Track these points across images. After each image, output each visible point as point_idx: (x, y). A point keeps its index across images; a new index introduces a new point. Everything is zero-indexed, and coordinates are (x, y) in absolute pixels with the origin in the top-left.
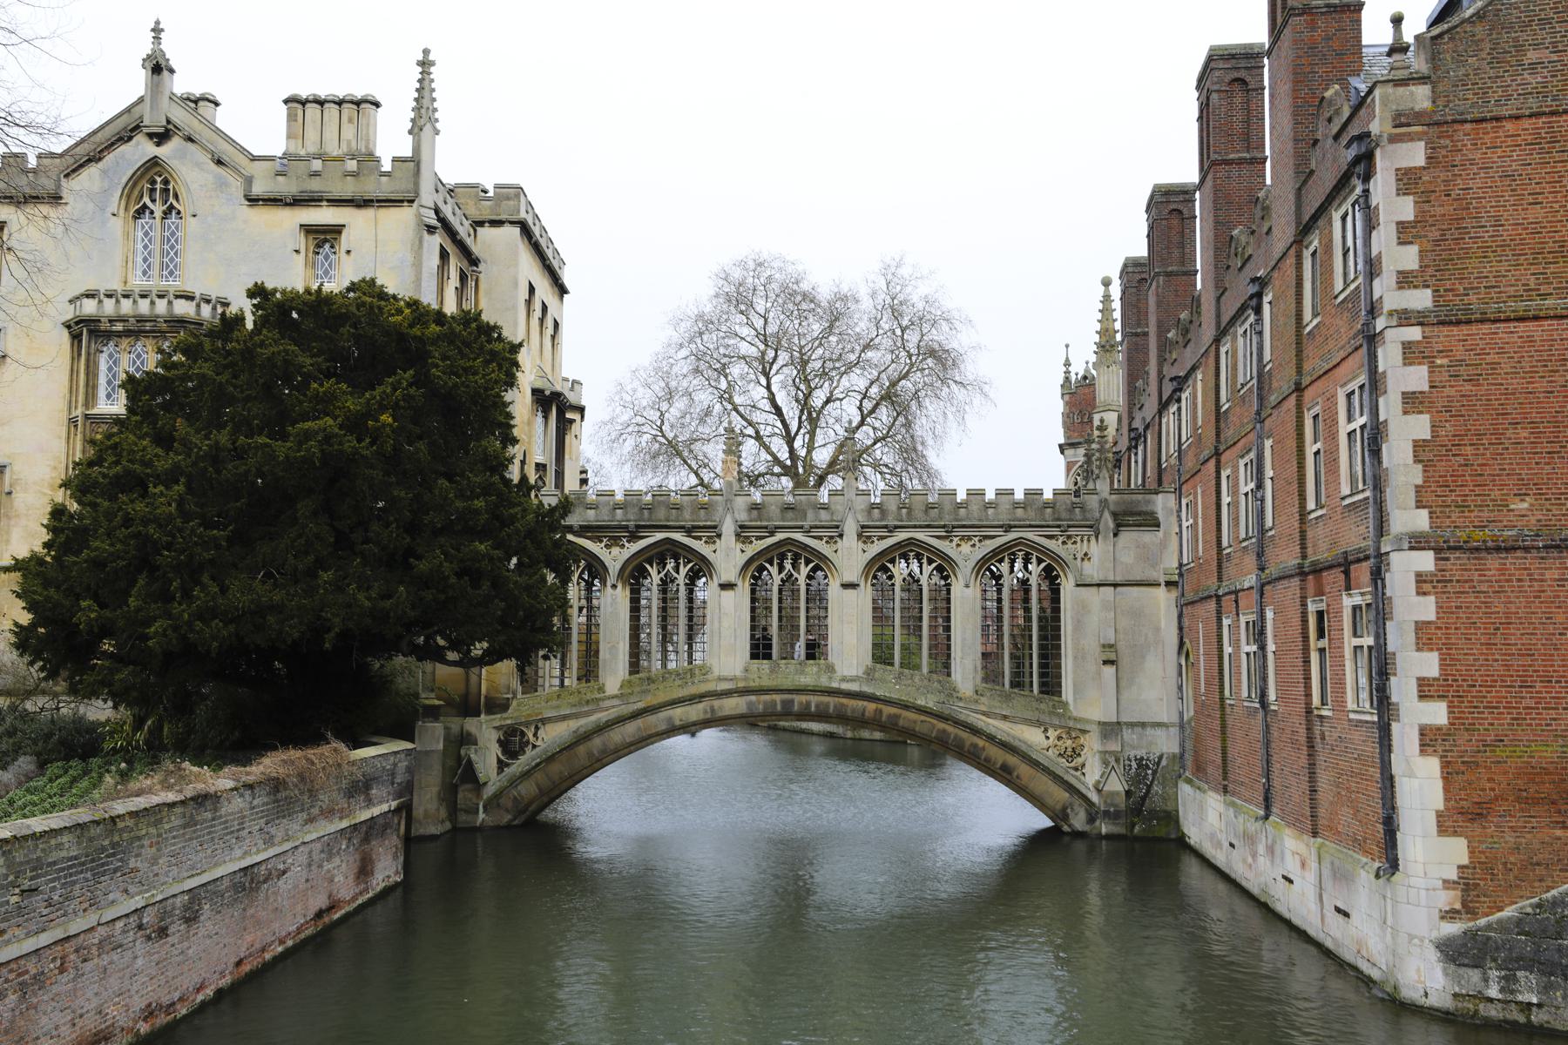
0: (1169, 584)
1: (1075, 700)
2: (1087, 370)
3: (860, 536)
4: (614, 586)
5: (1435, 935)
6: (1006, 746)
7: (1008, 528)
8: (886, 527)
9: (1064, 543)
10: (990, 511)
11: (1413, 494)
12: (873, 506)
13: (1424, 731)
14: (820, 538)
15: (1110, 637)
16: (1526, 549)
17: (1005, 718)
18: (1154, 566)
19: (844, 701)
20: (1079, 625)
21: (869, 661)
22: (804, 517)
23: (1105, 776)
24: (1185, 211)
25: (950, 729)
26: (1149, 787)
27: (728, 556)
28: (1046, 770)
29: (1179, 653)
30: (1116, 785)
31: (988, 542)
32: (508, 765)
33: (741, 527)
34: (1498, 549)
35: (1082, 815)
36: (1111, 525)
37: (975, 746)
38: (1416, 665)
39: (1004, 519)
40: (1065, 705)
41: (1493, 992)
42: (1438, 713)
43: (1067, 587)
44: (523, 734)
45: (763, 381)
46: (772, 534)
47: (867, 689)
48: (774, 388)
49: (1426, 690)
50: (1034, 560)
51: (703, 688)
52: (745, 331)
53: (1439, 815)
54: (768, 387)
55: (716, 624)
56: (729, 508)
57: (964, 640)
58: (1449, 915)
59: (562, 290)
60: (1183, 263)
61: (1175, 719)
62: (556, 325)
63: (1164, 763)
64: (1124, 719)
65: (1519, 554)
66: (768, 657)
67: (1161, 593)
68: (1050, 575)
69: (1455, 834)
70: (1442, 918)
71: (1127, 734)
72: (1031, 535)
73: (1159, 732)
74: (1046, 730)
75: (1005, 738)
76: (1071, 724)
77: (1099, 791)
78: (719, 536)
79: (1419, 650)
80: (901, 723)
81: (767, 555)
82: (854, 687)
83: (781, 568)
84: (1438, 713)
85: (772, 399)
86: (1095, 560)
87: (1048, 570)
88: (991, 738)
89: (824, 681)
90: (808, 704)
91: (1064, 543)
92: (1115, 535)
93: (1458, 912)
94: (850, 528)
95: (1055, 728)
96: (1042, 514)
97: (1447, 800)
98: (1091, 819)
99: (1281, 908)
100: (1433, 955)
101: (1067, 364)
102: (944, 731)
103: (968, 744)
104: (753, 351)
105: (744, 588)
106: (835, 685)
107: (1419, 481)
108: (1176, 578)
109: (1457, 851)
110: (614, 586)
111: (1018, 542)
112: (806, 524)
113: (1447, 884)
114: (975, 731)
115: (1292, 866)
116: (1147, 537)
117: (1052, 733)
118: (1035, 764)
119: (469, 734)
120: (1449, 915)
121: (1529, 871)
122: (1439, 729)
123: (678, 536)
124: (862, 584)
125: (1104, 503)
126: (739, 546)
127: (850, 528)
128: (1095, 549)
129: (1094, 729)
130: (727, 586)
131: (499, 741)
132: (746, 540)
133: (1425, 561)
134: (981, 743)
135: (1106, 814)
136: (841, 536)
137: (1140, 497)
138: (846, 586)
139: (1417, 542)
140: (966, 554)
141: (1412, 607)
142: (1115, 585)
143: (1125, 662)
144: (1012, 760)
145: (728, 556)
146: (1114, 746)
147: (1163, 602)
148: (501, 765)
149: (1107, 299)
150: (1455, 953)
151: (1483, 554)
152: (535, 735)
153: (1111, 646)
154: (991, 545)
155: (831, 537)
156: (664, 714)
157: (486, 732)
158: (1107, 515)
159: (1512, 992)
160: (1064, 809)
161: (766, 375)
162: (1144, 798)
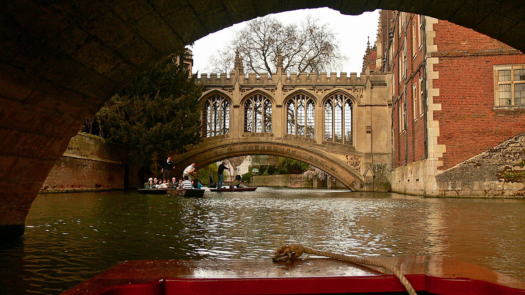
0: (389, 105)
1: (357, 146)
5: (436, 174)
7: (334, 86)
8: (292, 86)
11: (433, 40)
12: (287, 79)
13: (434, 112)
14: (269, 90)
16: (465, 56)
18: (384, 99)
19: (277, 146)
25: (314, 156)
26: (382, 175)
30: (370, 174)
31: (328, 91)
33: (241, 86)
34: (457, 56)
35: (359, 185)
37: (322, 161)
38: (433, 92)
41: (450, 188)
42: (438, 107)
43: (355, 106)
45: (263, 58)
46: (252, 88)
47: (285, 142)
48: (268, 60)
49: (436, 100)
51: (228, 142)
52: (257, 39)
53: (438, 138)
54: (265, 60)
56: (237, 80)
58: (440, 168)
65: (463, 58)
67: (387, 108)
69: (443, 144)
70: (438, 169)
71: (375, 157)
72: (342, 89)
73: (386, 156)
74: (347, 156)
75: (332, 159)
78: (234, 89)
79: (434, 88)
80: (296, 154)
82: (280, 141)
84: (438, 107)
85: (266, 64)
86: (365, 97)
88: (327, 159)
89: (270, 139)
90: (264, 147)
92: (371, 88)
93: (442, 167)
96: (347, 81)
97: (440, 133)
98: (362, 186)
100: (434, 179)
101: (369, 43)
103: (319, 161)
104: (259, 47)
107: (435, 37)
109: (443, 148)
111: (338, 91)
113: (440, 159)
114: (322, 156)
116: (383, 89)
117: (349, 157)
118: (343, 168)
120: (440, 168)
121: (464, 153)
122: (439, 112)
123: (219, 89)
125: (368, 78)
126: (241, 93)
127: (280, 87)
130: (236, 107)
133: (436, 60)
134: (324, 160)
135: (366, 183)
136: (276, 89)
138: (277, 106)
139: (434, 55)
141: (432, 75)
142: (371, 106)
143: (374, 131)
150: (440, 179)
151: (453, 58)
153: (369, 127)
154: (328, 92)
155: (273, 90)
156: (214, 151)
158: (369, 81)
159: (455, 187)
160: (353, 183)
161: (264, 55)
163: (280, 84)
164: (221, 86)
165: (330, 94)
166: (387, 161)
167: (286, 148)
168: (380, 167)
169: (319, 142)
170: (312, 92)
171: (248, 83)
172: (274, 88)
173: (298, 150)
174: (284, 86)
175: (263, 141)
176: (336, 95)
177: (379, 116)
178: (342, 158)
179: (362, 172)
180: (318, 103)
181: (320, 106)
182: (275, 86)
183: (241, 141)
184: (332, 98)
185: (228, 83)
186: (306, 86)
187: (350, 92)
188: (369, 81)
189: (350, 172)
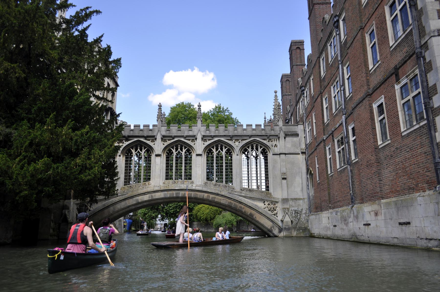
0: (302, 153)
1: (273, 192)
2: (271, 118)
3: (202, 139)
4: (120, 156)
6: (250, 207)
8: (211, 136)
9: (268, 141)
10: (245, 131)
14: (189, 140)
15: (284, 170)
17: (251, 198)
18: (297, 148)
20: (274, 167)
21: (205, 180)
23: (284, 217)
24: (301, 48)
25: (232, 202)
26: (299, 220)
27: (158, 146)
28: (264, 215)
29: (307, 174)
30: (287, 219)
33: (163, 136)
37: (241, 207)
39: (249, 133)
40: (270, 194)
43: (270, 156)
44: (86, 206)
46: (173, 139)
50: (259, 147)
51: (149, 189)
55: (154, 168)
57: (237, 172)
60: (301, 62)
61: (306, 196)
63: (304, 211)
64: (289, 197)
66: (171, 178)
71: (291, 202)
72: (258, 139)
73: (301, 201)
74: (264, 202)
76: (273, 200)
77: (282, 221)
78: (156, 139)
83: (177, 150)
86: (278, 146)
89: (190, 187)
90: (185, 194)
91: (268, 141)
92: (285, 138)
94: (199, 137)
95: (267, 201)
99: (365, 238)
101: (265, 118)
102: (231, 202)
105: (164, 157)
108: (305, 151)
110: (120, 156)
111: (254, 141)
114: (241, 203)
115: (369, 218)
116: (295, 139)
117: (267, 203)
118: (261, 213)
119: (66, 206)
123: (142, 139)
124: (203, 155)
125: (281, 129)
126: (162, 142)
127: (199, 137)
128: (277, 143)
129: (280, 200)
131: (77, 209)
132: (165, 141)
136: (196, 139)
137: (292, 127)
138: (197, 155)
142: (285, 154)
144: (253, 212)
145: (158, 146)
146: (286, 206)
147: (301, 158)
149: (276, 96)
153: (285, 173)
156: (135, 199)
160: (271, 228)
162: (297, 224)
163: (199, 134)
165: (247, 144)
166: (304, 206)
167: (206, 195)
168: (296, 212)
169: (238, 189)
170: (230, 142)
171: (169, 133)
172: (194, 138)
173: (217, 197)
174: (204, 136)
178: (260, 205)
179: (280, 217)
180: (235, 152)
181: (237, 155)
182: (195, 136)
183: (162, 189)
185: (150, 134)
186: (225, 136)
187: (265, 142)
188: (282, 132)
189: (268, 218)
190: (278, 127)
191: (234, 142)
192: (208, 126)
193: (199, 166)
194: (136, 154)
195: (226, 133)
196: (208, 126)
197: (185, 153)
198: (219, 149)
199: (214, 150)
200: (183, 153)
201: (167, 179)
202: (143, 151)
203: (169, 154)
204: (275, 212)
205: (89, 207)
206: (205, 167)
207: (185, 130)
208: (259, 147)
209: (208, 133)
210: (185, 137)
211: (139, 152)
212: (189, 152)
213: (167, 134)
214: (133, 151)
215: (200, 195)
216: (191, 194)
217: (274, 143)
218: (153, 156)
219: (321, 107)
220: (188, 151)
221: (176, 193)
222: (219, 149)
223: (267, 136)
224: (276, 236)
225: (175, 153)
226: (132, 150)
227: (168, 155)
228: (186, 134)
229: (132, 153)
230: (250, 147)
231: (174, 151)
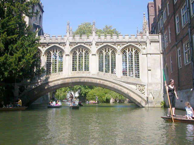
3: (96, 44)
8: (101, 42)
14: (87, 45)
22: (84, 40)
32: (21, 94)
36: (149, 42)
37: (121, 89)
44: (24, 87)
46: (77, 44)
50: (133, 49)
59: (43, 11)
62: (41, 16)
66: (76, 70)
68: (137, 53)
72: (132, 44)
74: (136, 85)
81: (76, 48)
83: (79, 51)
86: (146, 49)
87: (136, 51)
89: (88, 75)
90: (85, 80)
92: (150, 44)
98: (146, 104)
105: (71, 56)
106: (90, 76)
111: (130, 45)
112: (84, 42)
114: (121, 86)
132: (72, 46)
136: (92, 44)
138: (92, 55)
140: (119, 48)
142: (151, 54)
145: (67, 49)
148: (19, 94)
152: (27, 87)
155: (90, 45)
157: (17, 86)
163: (94, 41)
164: (58, 43)
165: (125, 47)
167: (98, 81)
170: (114, 46)
172: (90, 44)
174: (97, 42)
175: (84, 76)
176: (129, 48)
177: (155, 60)
178: (133, 87)
181: (119, 55)
183: (70, 76)
184: (126, 50)
187: (137, 46)
188: (148, 39)
190: (146, 36)
191: (117, 46)
192: (99, 36)
193: (94, 62)
194: (53, 54)
195: (111, 40)
196: (99, 36)
197: (85, 53)
198: (107, 51)
199: (104, 52)
200: (83, 54)
201: (73, 70)
202: (58, 52)
203: (75, 54)
204: (143, 92)
205: (25, 87)
206: (98, 63)
207: (84, 39)
208: (133, 49)
209: (99, 41)
210: (84, 44)
211: (55, 53)
212: (87, 52)
213: (73, 41)
214: (52, 52)
215: (94, 81)
216: (89, 80)
217: (143, 47)
218: (64, 56)
219: (174, 23)
220: (87, 52)
221: (79, 80)
222: (107, 51)
223: (138, 42)
224: (144, 107)
225: (78, 54)
226: (51, 52)
227: (74, 55)
228: (85, 41)
229: (51, 54)
230: (127, 49)
231: (77, 52)
